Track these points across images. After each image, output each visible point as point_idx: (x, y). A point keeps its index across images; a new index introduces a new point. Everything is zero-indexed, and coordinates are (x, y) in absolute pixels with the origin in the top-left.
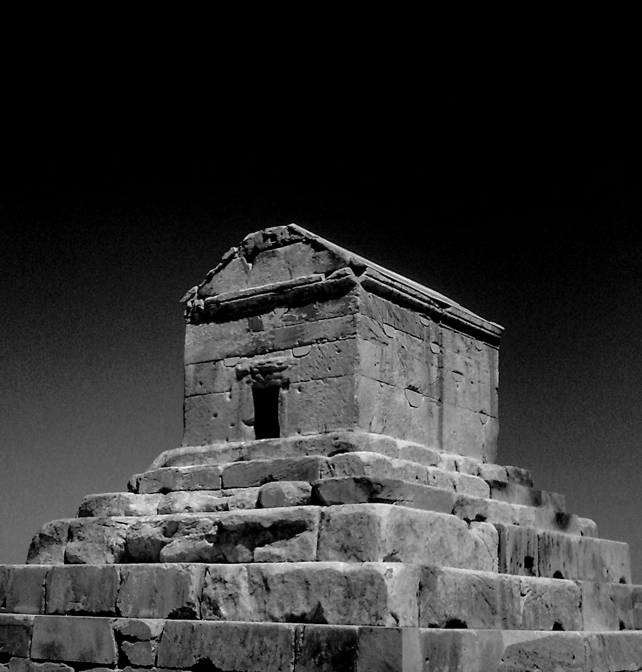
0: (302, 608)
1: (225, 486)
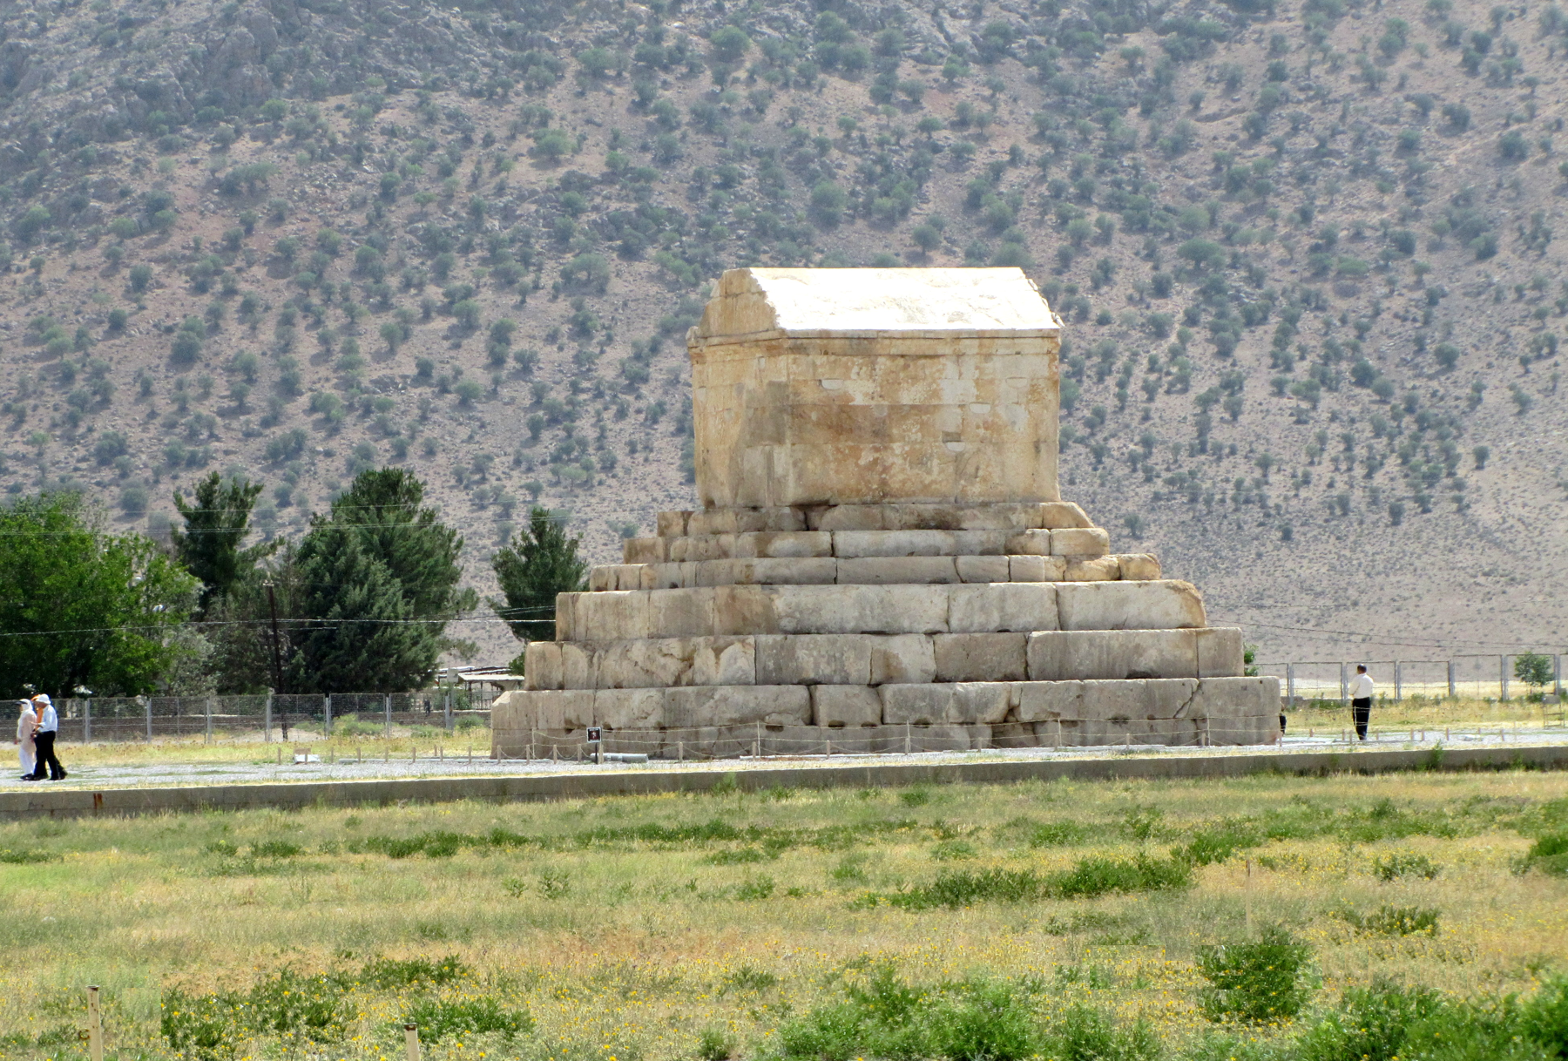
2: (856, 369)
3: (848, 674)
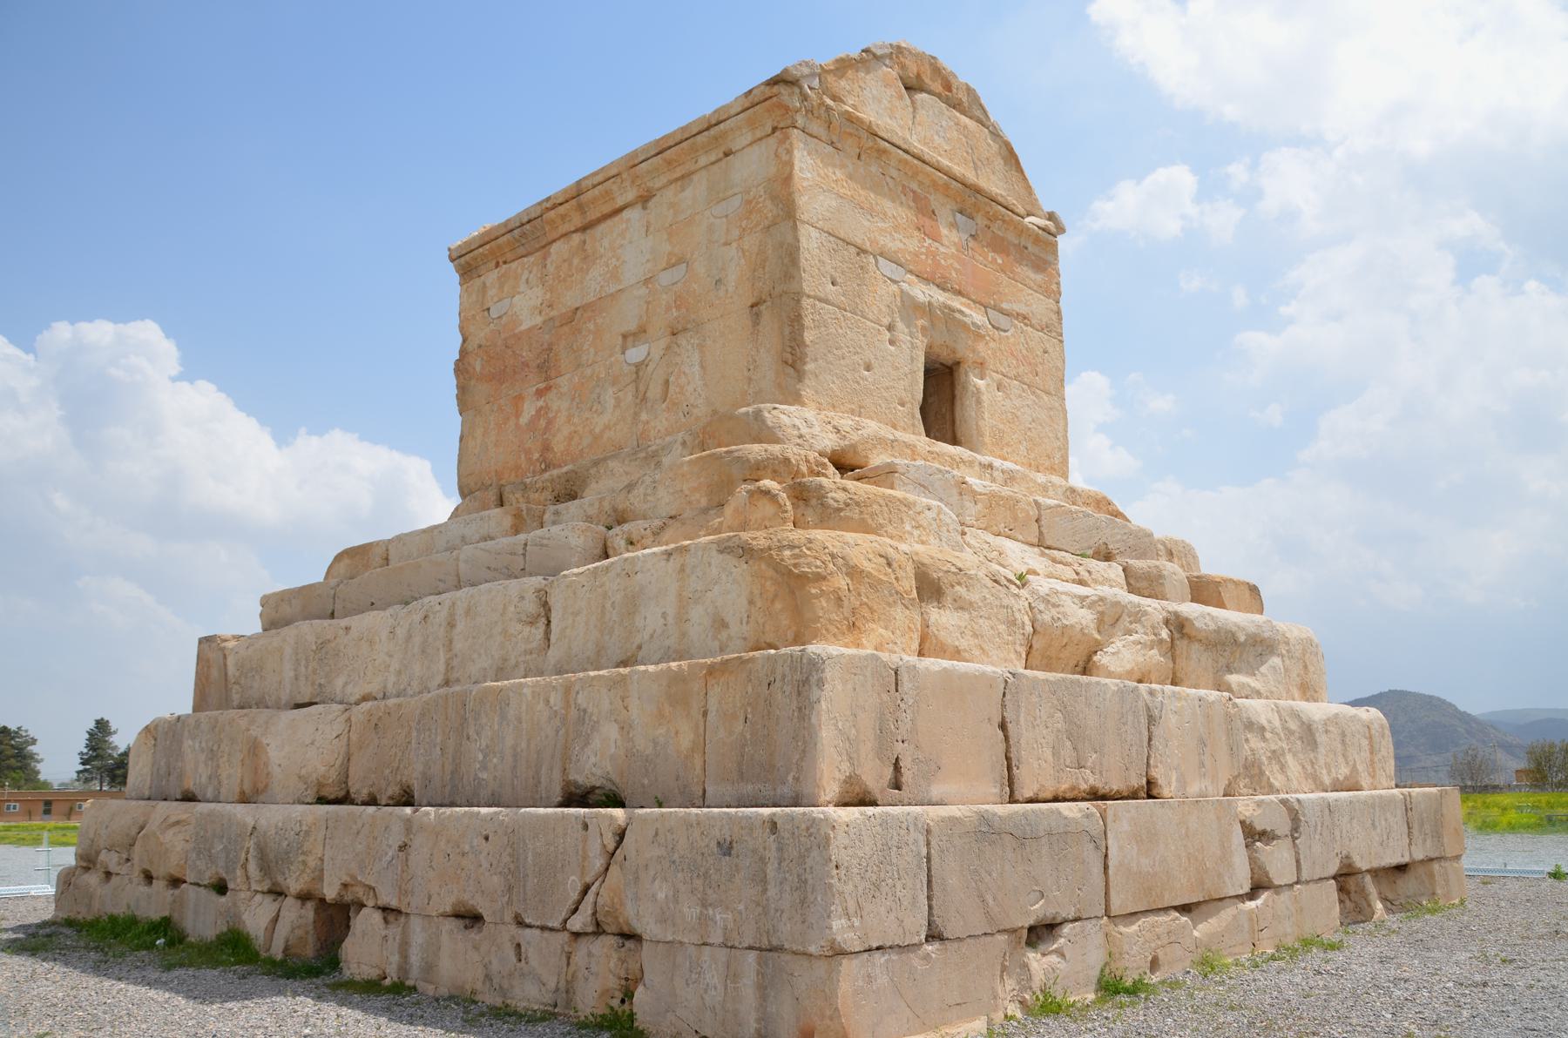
0: (1343, 771)
1: (1049, 543)
2: (524, 278)
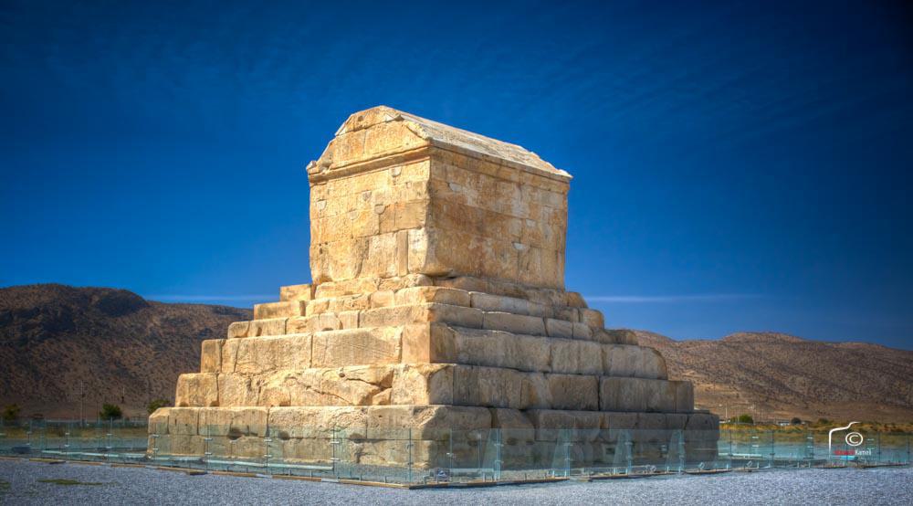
2: (468, 180)
3: (509, 400)
